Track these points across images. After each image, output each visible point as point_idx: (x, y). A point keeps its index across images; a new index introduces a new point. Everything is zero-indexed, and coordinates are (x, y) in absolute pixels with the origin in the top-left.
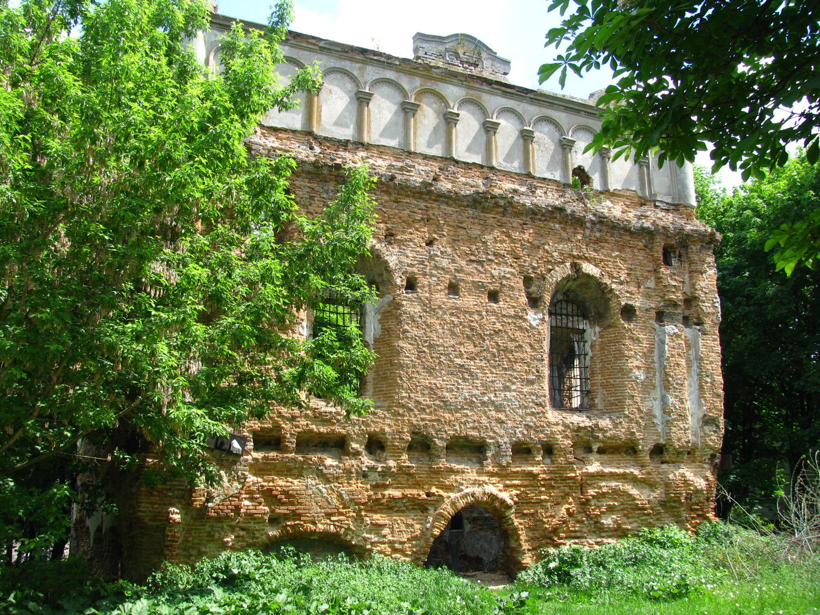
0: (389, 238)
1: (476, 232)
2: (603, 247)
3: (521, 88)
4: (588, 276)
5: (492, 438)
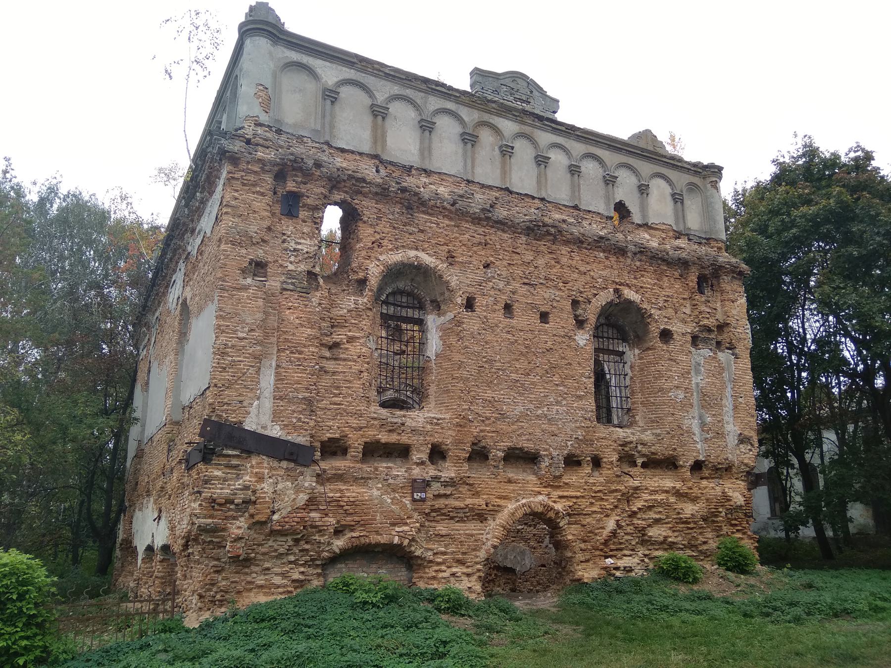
0: (450, 260)
1: (529, 257)
2: (642, 276)
3: (569, 125)
4: (630, 302)
5: (546, 450)
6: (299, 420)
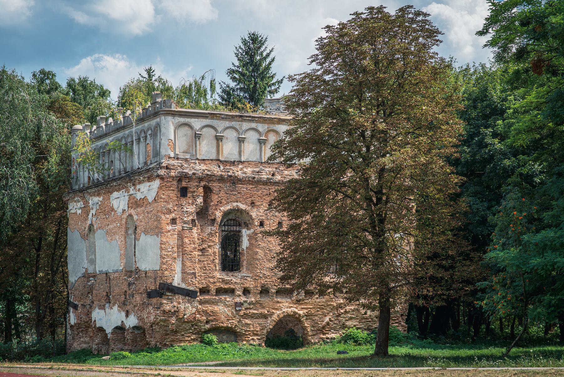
6: (191, 281)
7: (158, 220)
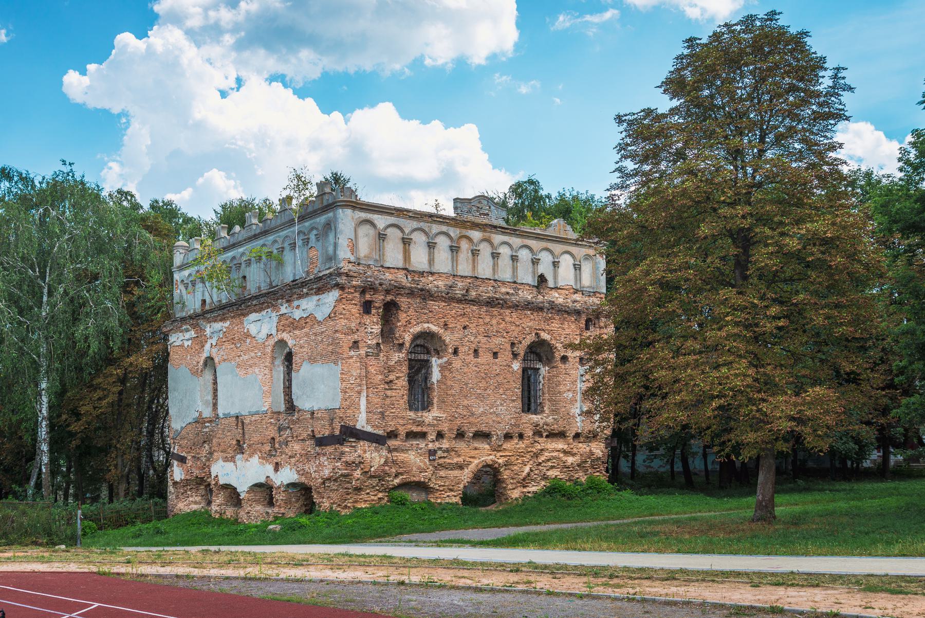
4: (544, 341)
7: (335, 342)
